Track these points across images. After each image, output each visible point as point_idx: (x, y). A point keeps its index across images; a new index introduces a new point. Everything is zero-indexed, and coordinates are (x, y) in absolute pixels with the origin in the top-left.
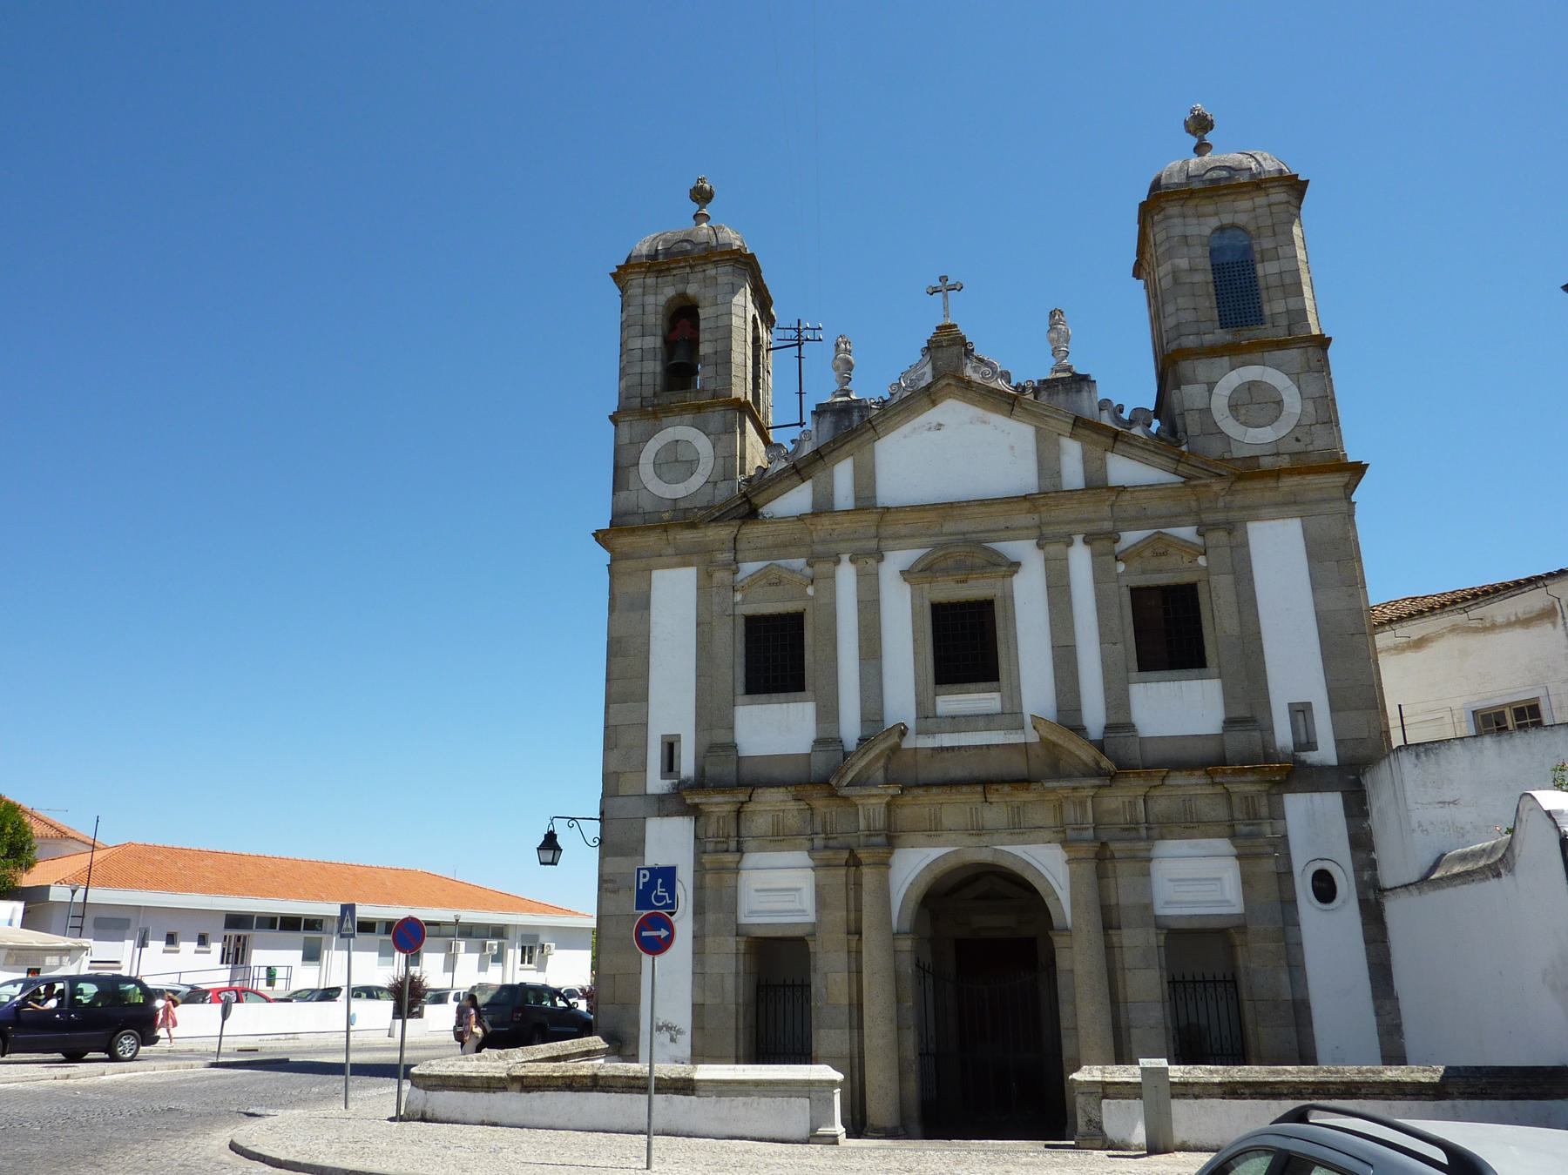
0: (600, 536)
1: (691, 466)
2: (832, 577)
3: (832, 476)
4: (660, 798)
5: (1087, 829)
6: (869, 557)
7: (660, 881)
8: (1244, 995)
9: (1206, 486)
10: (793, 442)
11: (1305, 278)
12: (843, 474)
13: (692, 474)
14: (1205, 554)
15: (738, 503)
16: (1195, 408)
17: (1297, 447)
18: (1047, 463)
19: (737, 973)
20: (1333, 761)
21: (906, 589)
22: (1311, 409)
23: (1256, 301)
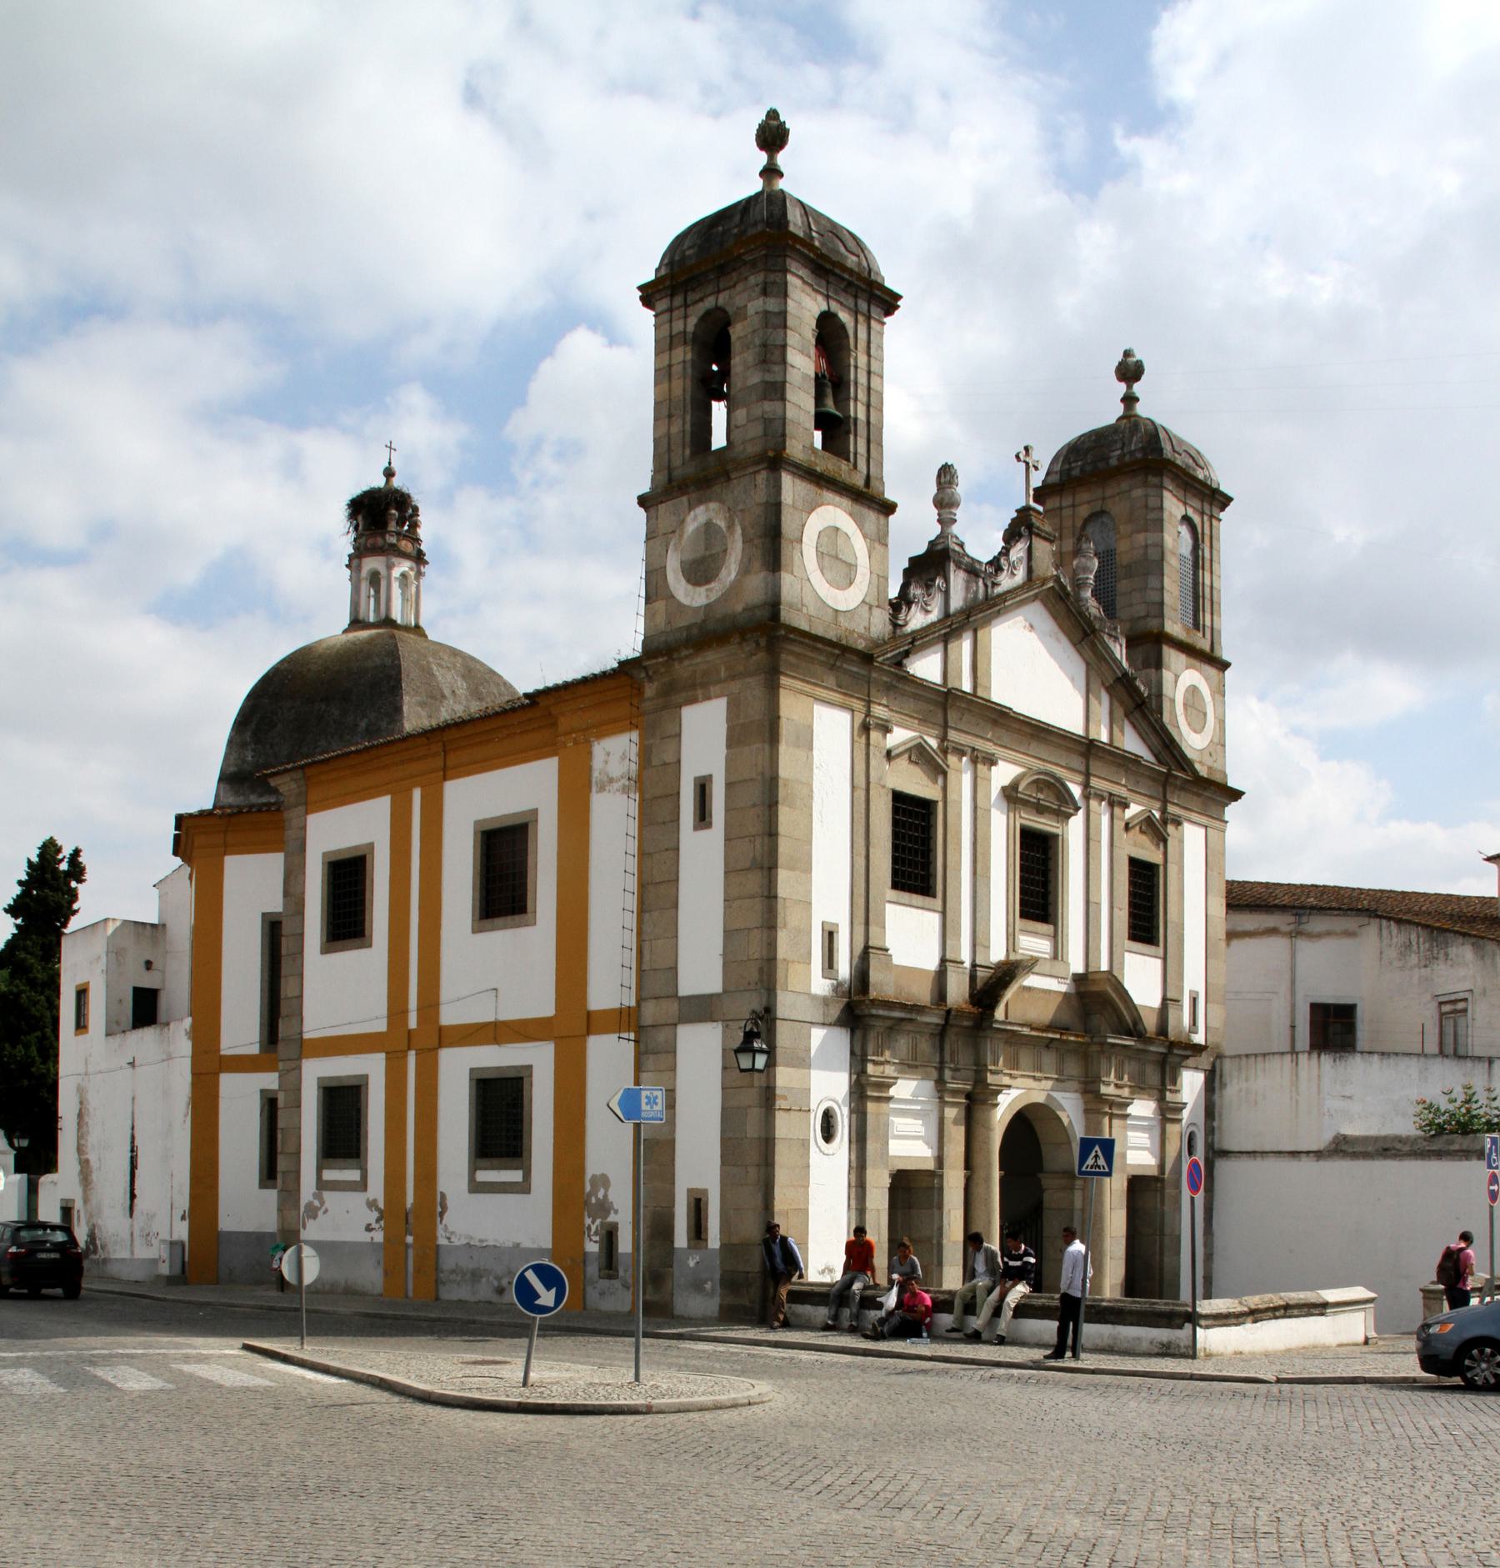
13: (851, 584)
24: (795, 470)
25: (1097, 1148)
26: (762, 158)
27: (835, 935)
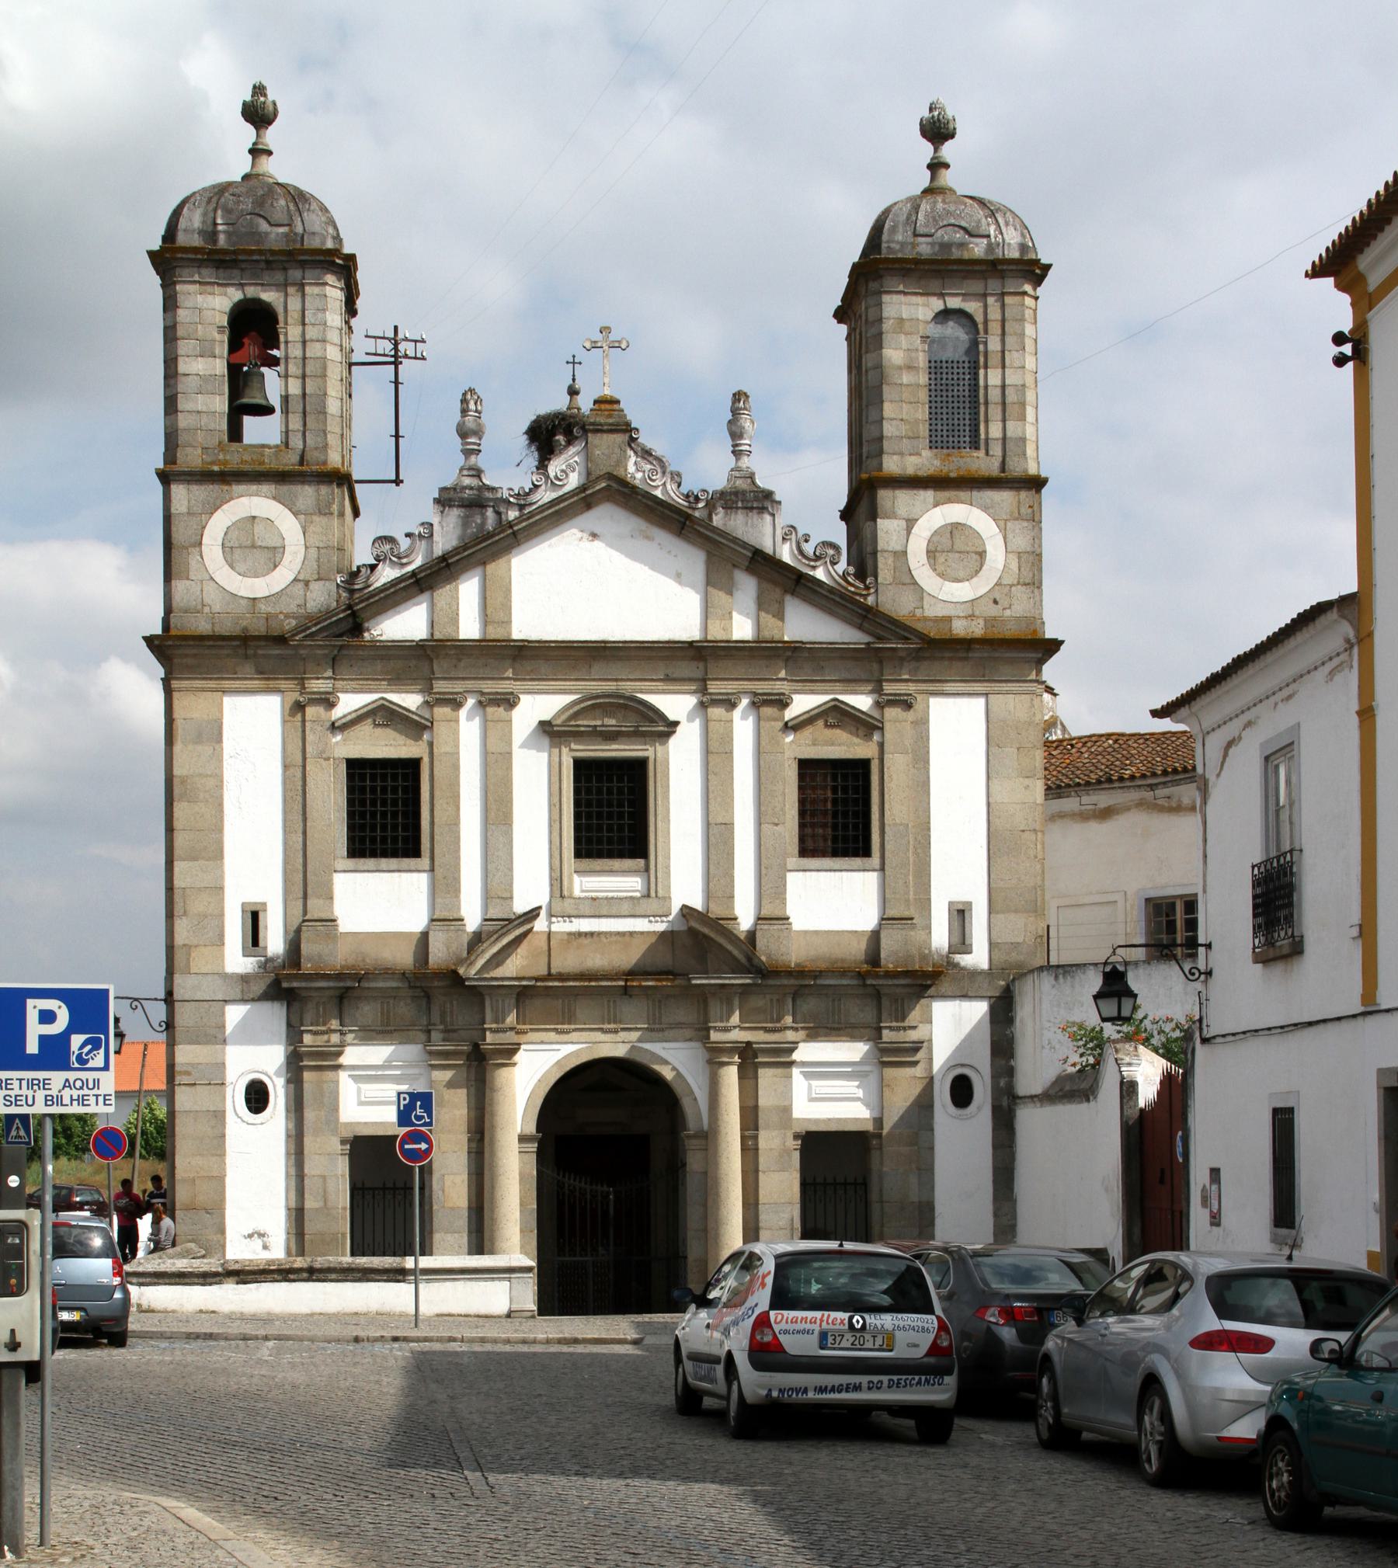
1: (274, 555)
4: (244, 979)
7: (419, 1103)
8: (874, 1196)
10: (408, 535)
11: (1030, 396)
13: (275, 566)
16: (890, 549)
17: (993, 611)
20: (985, 966)
22: (1014, 566)
24: (189, 478)
25: (17, 1121)
26: (249, 132)
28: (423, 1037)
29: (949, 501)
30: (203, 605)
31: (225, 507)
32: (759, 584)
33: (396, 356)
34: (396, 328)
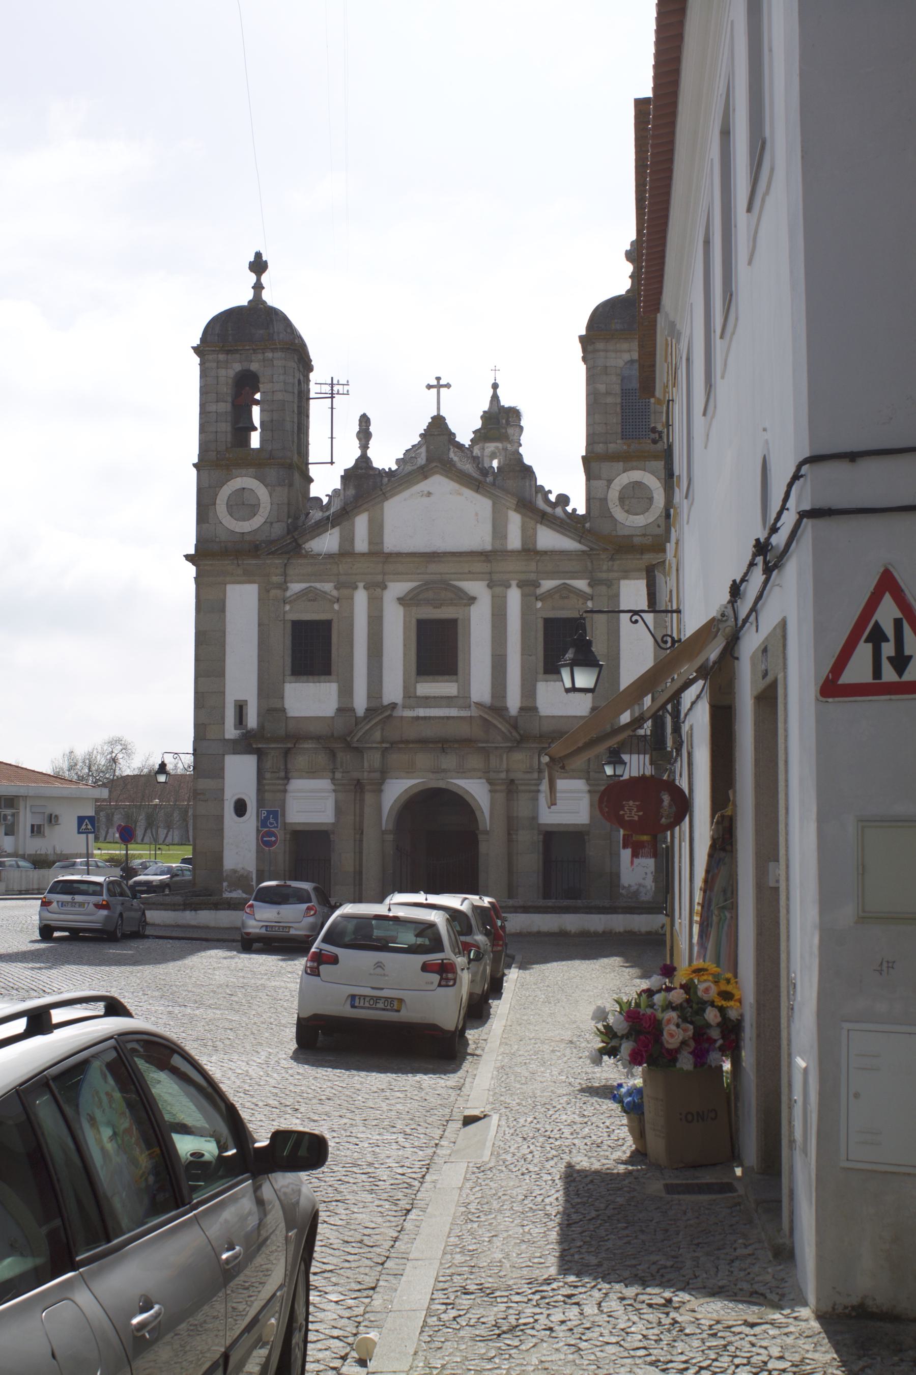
0: (188, 557)
1: (253, 509)
2: (351, 598)
3: (353, 525)
4: (234, 742)
5: (502, 772)
6: (376, 588)
9: (598, 554)
12: (361, 523)
13: (255, 515)
14: (592, 599)
15: (288, 542)
18: (499, 529)
19: (285, 852)
21: (400, 611)
23: (647, 420)
25: (87, 821)
26: (253, 278)
27: (244, 707)
28: (330, 775)
29: (632, 469)
30: (216, 537)
31: (228, 483)
32: (522, 518)
33: (332, 394)
34: (332, 378)
